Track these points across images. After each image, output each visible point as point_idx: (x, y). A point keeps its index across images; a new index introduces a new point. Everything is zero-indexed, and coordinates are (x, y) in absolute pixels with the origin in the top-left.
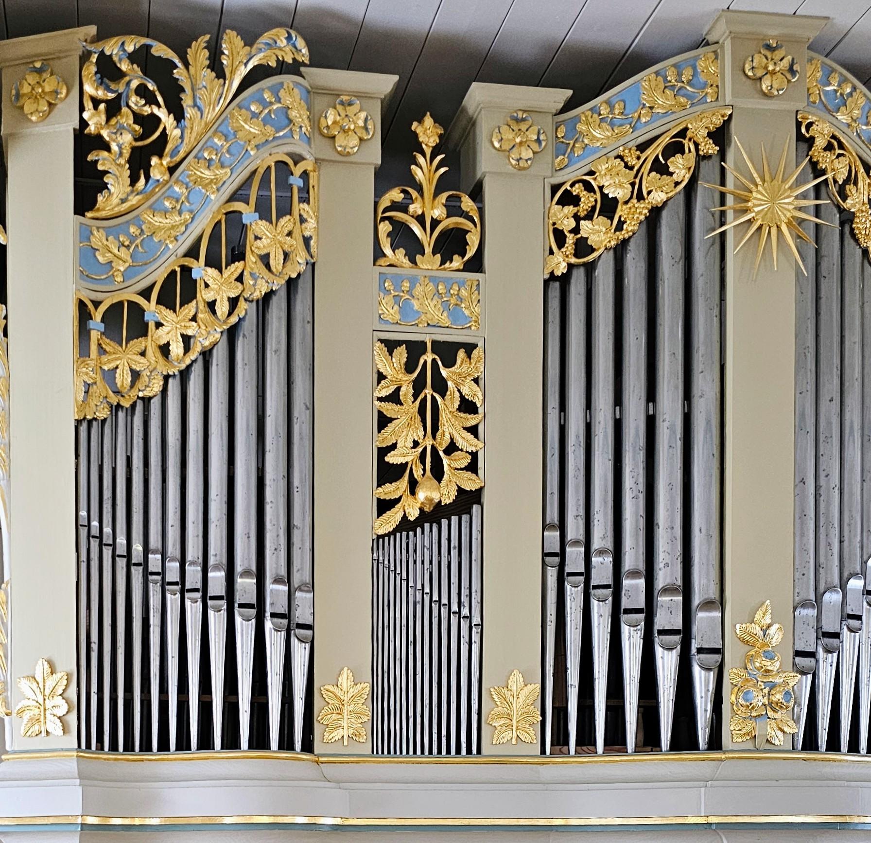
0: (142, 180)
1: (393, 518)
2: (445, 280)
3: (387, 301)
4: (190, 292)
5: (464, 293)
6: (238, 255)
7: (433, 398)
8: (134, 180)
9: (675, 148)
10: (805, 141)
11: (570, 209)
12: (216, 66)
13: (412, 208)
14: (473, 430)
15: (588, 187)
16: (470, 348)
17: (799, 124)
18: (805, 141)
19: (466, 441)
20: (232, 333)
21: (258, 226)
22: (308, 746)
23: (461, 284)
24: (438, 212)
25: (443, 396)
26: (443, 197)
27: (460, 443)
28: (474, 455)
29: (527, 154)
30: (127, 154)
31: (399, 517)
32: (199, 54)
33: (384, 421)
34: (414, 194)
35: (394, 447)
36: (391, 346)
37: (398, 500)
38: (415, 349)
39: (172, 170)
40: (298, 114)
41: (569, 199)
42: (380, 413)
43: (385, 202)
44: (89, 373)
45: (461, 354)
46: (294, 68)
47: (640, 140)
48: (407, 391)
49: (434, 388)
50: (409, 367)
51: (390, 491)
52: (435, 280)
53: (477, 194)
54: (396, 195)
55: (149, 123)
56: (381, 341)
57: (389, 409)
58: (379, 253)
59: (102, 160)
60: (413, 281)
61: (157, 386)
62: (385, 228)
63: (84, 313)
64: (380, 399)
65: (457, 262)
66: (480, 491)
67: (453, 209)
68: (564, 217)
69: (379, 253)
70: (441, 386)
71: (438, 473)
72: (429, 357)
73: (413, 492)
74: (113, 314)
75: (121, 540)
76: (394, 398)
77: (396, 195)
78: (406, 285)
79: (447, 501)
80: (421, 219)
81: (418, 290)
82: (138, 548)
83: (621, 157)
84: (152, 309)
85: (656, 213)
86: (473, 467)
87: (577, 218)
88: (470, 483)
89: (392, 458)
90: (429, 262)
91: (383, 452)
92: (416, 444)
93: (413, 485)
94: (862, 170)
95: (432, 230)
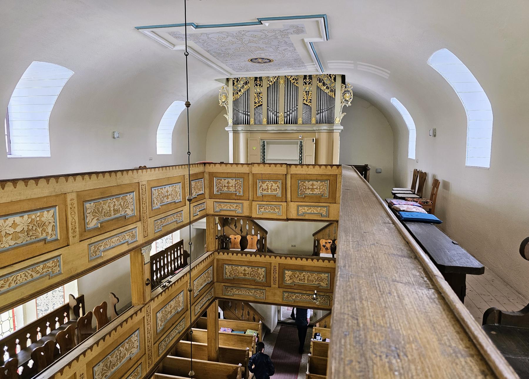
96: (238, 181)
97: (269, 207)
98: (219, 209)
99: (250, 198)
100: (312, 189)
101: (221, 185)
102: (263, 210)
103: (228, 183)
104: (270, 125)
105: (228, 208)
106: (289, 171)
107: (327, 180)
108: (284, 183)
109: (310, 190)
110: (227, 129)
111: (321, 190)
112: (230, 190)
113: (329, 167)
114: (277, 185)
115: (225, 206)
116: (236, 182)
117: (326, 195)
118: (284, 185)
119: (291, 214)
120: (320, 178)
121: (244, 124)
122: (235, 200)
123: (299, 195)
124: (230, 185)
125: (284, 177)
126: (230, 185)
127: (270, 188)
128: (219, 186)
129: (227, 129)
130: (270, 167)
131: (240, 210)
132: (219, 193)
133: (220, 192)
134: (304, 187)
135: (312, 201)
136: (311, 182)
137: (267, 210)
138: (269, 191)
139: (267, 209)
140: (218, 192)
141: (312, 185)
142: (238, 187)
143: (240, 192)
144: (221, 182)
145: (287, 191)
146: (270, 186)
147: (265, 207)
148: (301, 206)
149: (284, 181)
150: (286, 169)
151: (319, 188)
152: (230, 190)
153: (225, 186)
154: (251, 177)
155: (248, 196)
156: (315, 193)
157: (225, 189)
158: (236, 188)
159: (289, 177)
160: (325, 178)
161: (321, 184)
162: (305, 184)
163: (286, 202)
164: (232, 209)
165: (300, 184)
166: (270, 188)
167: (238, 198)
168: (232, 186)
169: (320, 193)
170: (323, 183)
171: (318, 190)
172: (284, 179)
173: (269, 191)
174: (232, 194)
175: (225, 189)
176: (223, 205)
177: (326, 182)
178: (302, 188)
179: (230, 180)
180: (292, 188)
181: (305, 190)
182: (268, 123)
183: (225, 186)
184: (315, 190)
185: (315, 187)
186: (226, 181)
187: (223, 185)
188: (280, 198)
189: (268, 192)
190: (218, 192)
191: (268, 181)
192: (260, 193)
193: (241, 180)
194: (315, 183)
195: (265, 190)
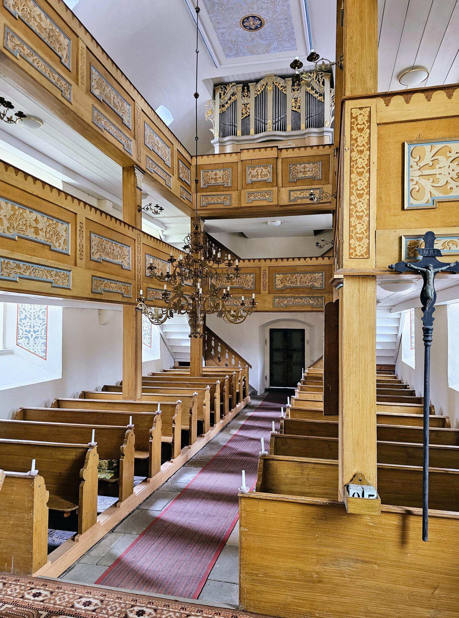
1: (243, 118)
4: (228, 102)
6: (231, 99)
10: (273, 83)
12: (229, 86)
18: (273, 83)
19: (249, 111)
20: (230, 105)
21: (232, 97)
22: (236, 135)
32: (228, 86)
33: (242, 110)
38: (245, 104)
40: (235, 89)
44: (220, 110)
46: (235, 85)
53: (250, 92)
55: (225, 91)
59: (221, 95)
63: (220, 106)
67: (248, 93)
68: (256, 92)
70: (247, 107)
71: (246, 114)
74: (222, 105)
84: (225, 105)
85: (262, 91)
86: (249, 113)
88: (249, 114)
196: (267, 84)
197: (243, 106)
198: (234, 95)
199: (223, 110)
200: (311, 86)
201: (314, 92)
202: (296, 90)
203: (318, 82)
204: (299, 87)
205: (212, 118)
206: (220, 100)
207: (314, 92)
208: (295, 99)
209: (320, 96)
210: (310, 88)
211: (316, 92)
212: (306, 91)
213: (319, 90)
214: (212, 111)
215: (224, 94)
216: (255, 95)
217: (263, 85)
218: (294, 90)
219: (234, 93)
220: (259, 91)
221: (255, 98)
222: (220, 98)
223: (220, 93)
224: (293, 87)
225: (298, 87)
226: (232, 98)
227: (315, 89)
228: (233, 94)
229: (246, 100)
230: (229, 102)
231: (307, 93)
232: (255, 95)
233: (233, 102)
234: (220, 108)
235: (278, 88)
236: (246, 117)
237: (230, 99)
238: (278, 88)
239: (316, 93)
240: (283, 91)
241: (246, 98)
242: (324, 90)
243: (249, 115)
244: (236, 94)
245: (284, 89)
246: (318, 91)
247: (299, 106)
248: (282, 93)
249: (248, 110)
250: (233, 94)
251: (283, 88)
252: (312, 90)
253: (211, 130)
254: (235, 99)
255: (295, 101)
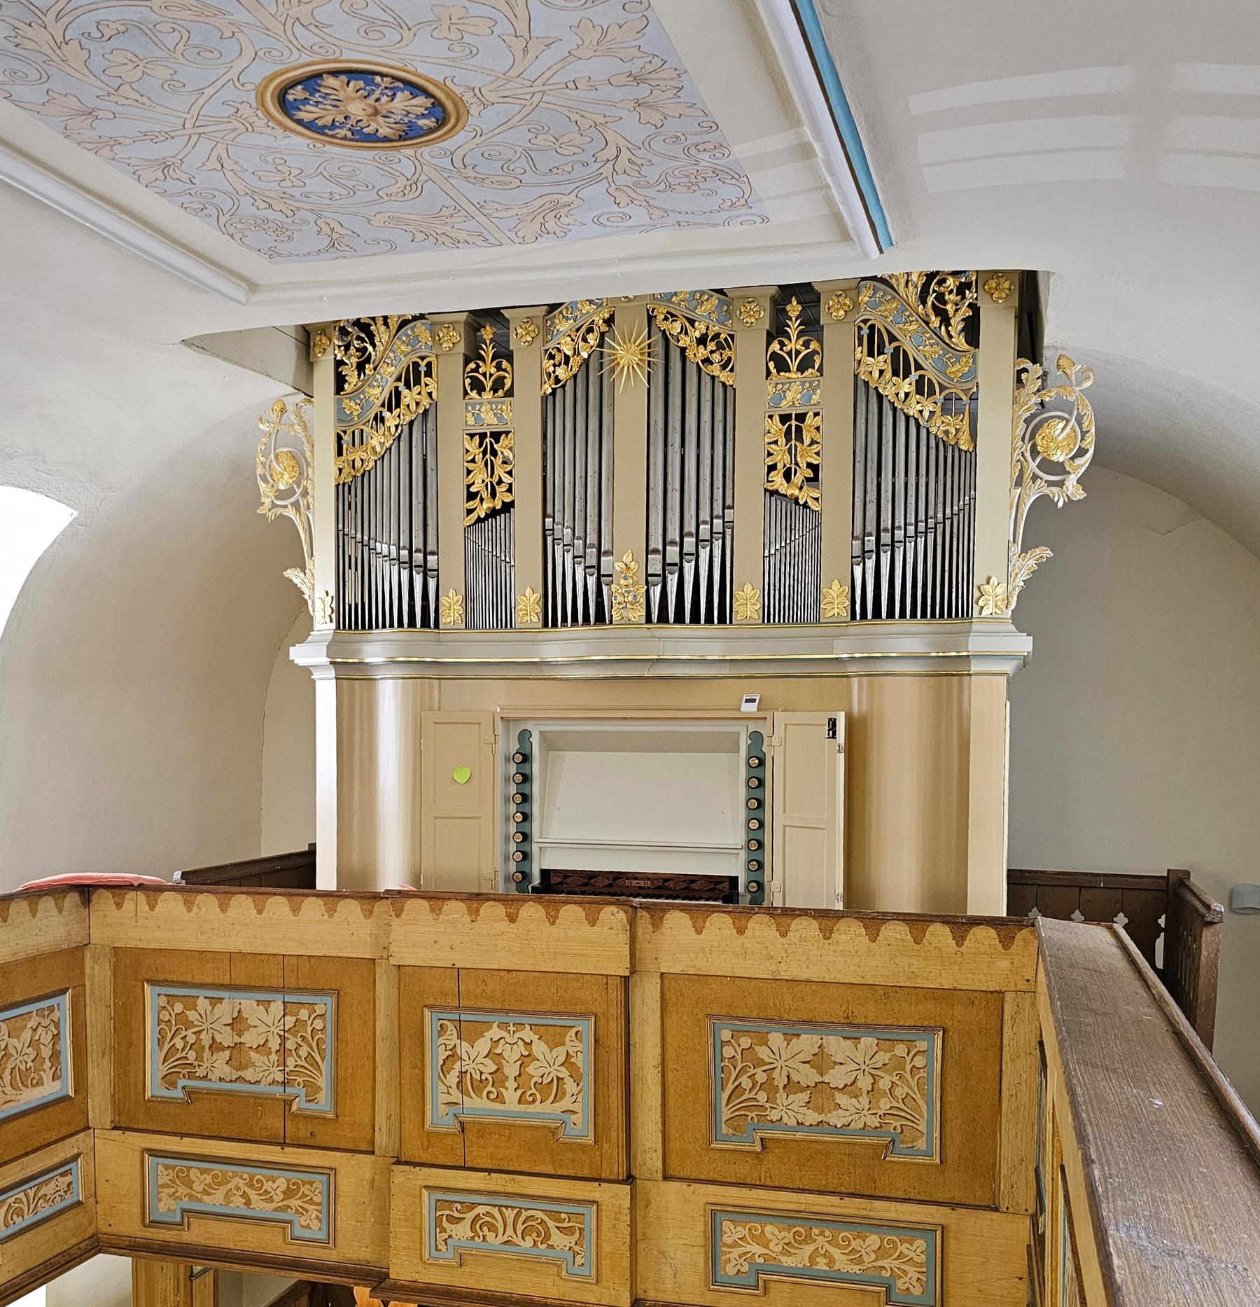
0: (362, 375)
1: (474, 516)
2: (496, 403)
3: (469, 415)
5: (504, 407)
7: (491, 460)
8: (359, 376)
9: (590, 330)
11: (552, 362)
13: (480, 370)
14: (510, 473)
15: (559, 350)
16: (507, 433)
17: (648, 310)
23: (503, 403)
24: (493, 370)
25: (495, 458)
26: (494, 363)
27: (504, 479)
28: (510, 485)
29: (529, 339)
30: (354, 366)
31: (476, 517)
33: (469, 472)
34: (481, 363)
35: (473, 483)
36: (472, 436)
37: (475, 509)
38: (483, 436)
39: (375, 369)
41: (552, 357)
42: (468, 469)
43: (468, 370)
45: (503, 437)
47: (577, 327)
48: (479, 457)
49: (491, 454)
50: (480, 446)
51: (471, 504)
52: (490, 403)
54: (472, 365)
56: (467, 434)
57: (471, 466)
58: (466, 393)
60: (481, 404)
61: (372, 464)
62: (468, 381)
64: (468, 462)
65: (500, 393)
66: (513, 501)
67: (499, 367)
68: (548, 365)
69: (466, 393)
70: (494, 453)
71: (493, 495)
72: (488, 440)
73: (482, 504)
75: (359, 536)
76: (473, 461)
77: (472, 365)
78: (478, 407)
79: (498, 507)
80: (484, 375)
81: (483, 409)
82: (366, 538)
83: (570, 336)
86: (510, 490)
87: (554, 365)
89: (473, 489)
90: (487, 395)
91: (469, 486)
92: (483, 481)
93: (482, 500)
94: (688, 325)
95: (490, 378)
96: (304, 1014)
97: (510, 1214)
98: (174, 1205)
99: (381, 1139)
100: (820, 1094)
101: (191, 1039)
102: (462, 1231)
103: (237, 1023)
104: (561, 631)
105: (237, 1202)
106: (647, 951)
107: (925, 1029)
108: (616, 1043)
109: (805, 1096)
110: (300, 655)
111: (885, 1104)
112: (248, 1074)
113: (940, 934)
114: (560, 1053)
115: (219, 1182)
116: (290, 1021)
117: (921, 1144)
118: (616, 1058)
119: (668, 1272)
120: (870, 1012)
121: (401, 625)
122: (283, 1145)
123: (725, 1129)
124: (251, 1039)
125: (615, 994)
126: (251, 1039)
127: (511, 1070)
128: (179, 1043)
129: (300, 655)
130: (512, 919)
131: (310, 1224)
132: (178, 1093)
133: (181, 1083)
134: (761, 1077)
135: (820, 1183)
136: (807, 1043)
137: (490, 1236)
138: (511, 1095)
139: (493, 1228)
140: (173, 1085)
141: (820, 1061)
142: (304, 1052)
143: (311, 1088)
144: (192, 1015)
145: (637, 1100)
146: (512, 1055)
147: (480, 1210)
148: (741, 1214)
149: (614, 1027)
150: (624, 938)
151: (865, 1083)
152: (248, 1074)
153: (215, 1047)
154: (384, 987)
155: (367, 1120)
156: (836, 1119)
157: (219, 1067)
158: (291, 1062)
159: (647, 996)
160: (912, 1012)
161: (884, 1057)
162: (763, 1052)
163: (630, 1179)
164: (261, 1207)
165: (728, 1052)
166: (511, 1070)
167: (303, 1131)
168: (262, 1048)
169: (874, 1122)
170: (901, 1050)
171: (864, 1100)
172: (616, 1011)
173: (511, 1095)
174: (259, 1099)
175: (219, 1067)
176: (199, 1177)
177: (922, 1045)
178: (745, 1082)
179: (247, 1004)
180: (670, 1077)
181: (762, 1097)
182: (550, 619)
183: (215, 1047)
184: (841, 1099)
185: (836, 1078)
186: (224, 1012)
187: (206, 1041)
188: (583, 1147)
189: (500, 1099)
190: (173, 1085)
191: (503, 1026)
192: (443, 1109)
193: (324, 1005)
194: (836, 1045)
195: (479, 1086)
196: (610, 321)
197: (473, 446)
198: (417, 382)
199: (358, 464)
200: (889, 349)
201: (907, 386)
202: (794, 366)
203: (935, 321)
204: (814, 345)
205: (296, 505)
206: (339, 403)
207: (907, 386)
208: (785, 418)
209: (945, 411)
210: (882, 362)
211: (922, 387)
212: (856, 376)
213: (942, 371)
214: (300, 465)
215: (361, 368)
216: (543, 383)
217: (590, 330)
218: (782, 366)
219: (416, 365)
220: (567, 358)
221: (545, 398)
222: (339, 387)
223: (339, 363)
224: (775, 346)
225: (806, 344)
226: (408, 397)
227: (919, 367)
228: (413, 376)
229: (488, 412)
230: (391, 419)
231: (861, 387)
232: (543, 383)
233: (411, 423)
234: (340, 453)
235: (683, 350)
236: (493, 513)
237: (394, 400)
238: (683, 350)
239: (919, 391)
240: (715, 369)
241: (487, 395)
242: (973, 372)
243: (508, 507)
244: (429, 374)
245: (716, 357)
246: (931, 374)
247: (814, 468)
248: (706, 381)
249: (500, 471)
250: (413, 376)
251: (712, 346)
252: (895, 373)
253: (293, 575)
254: (426, 402)
255: (788, 434)
